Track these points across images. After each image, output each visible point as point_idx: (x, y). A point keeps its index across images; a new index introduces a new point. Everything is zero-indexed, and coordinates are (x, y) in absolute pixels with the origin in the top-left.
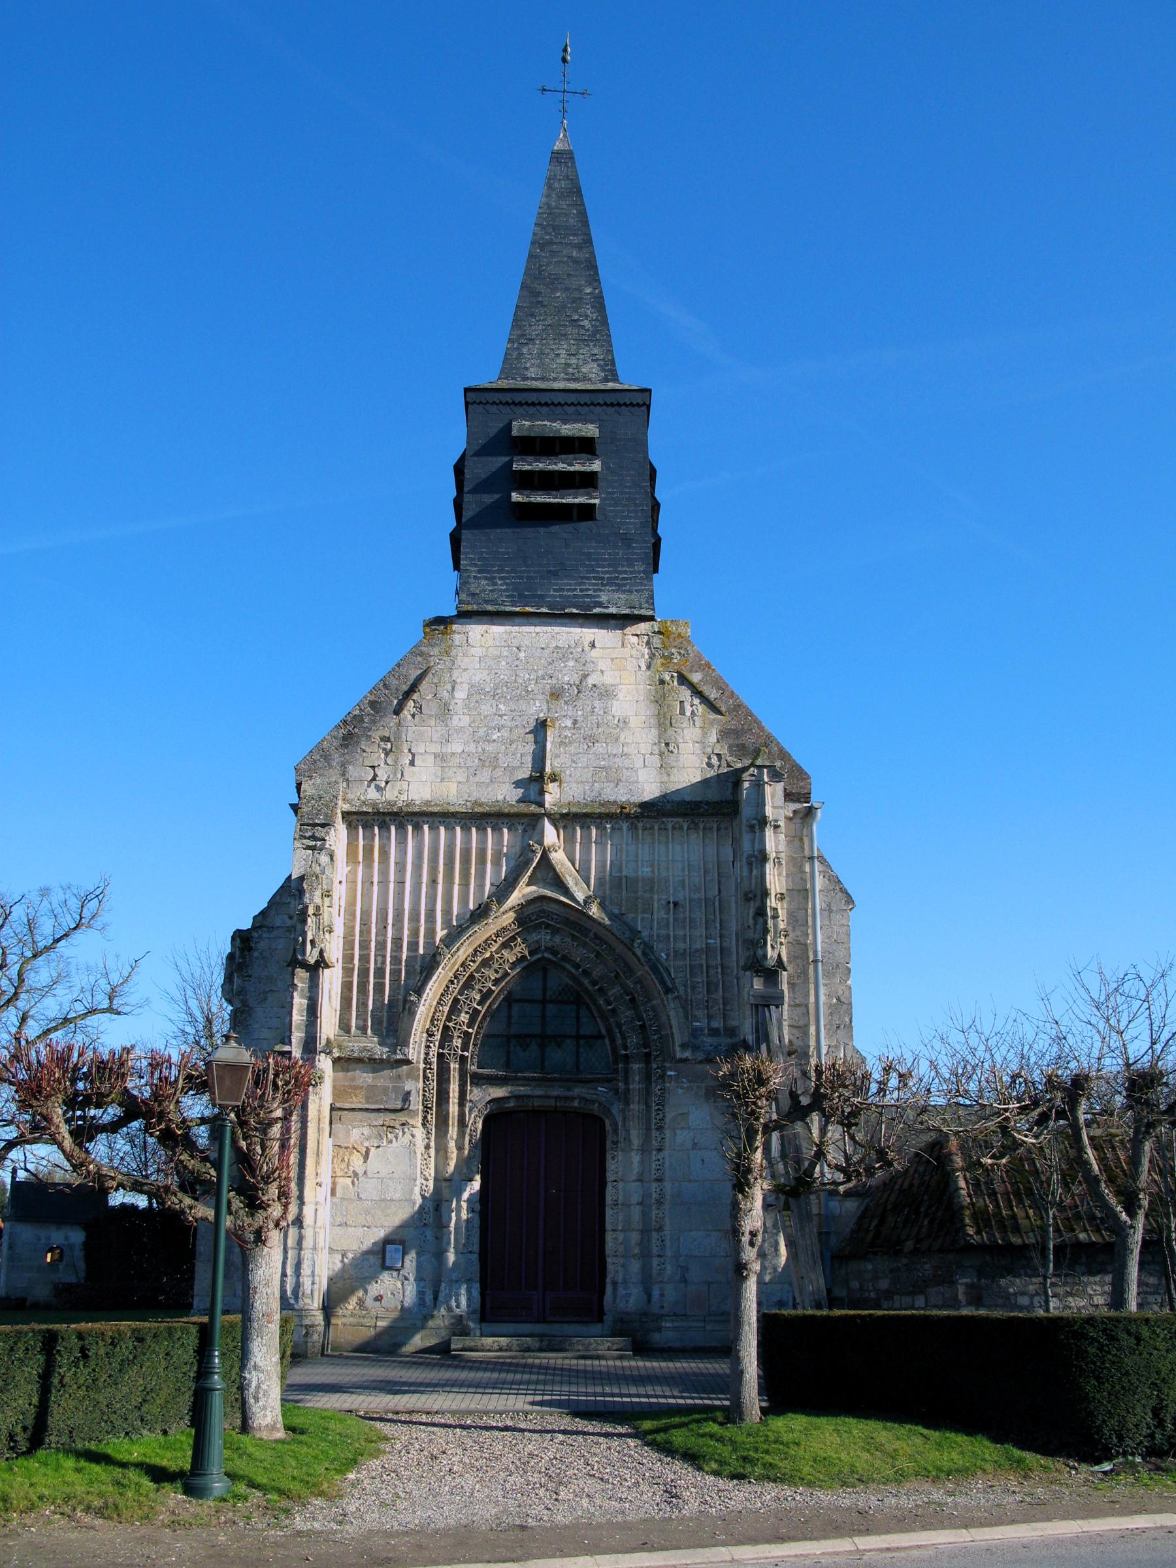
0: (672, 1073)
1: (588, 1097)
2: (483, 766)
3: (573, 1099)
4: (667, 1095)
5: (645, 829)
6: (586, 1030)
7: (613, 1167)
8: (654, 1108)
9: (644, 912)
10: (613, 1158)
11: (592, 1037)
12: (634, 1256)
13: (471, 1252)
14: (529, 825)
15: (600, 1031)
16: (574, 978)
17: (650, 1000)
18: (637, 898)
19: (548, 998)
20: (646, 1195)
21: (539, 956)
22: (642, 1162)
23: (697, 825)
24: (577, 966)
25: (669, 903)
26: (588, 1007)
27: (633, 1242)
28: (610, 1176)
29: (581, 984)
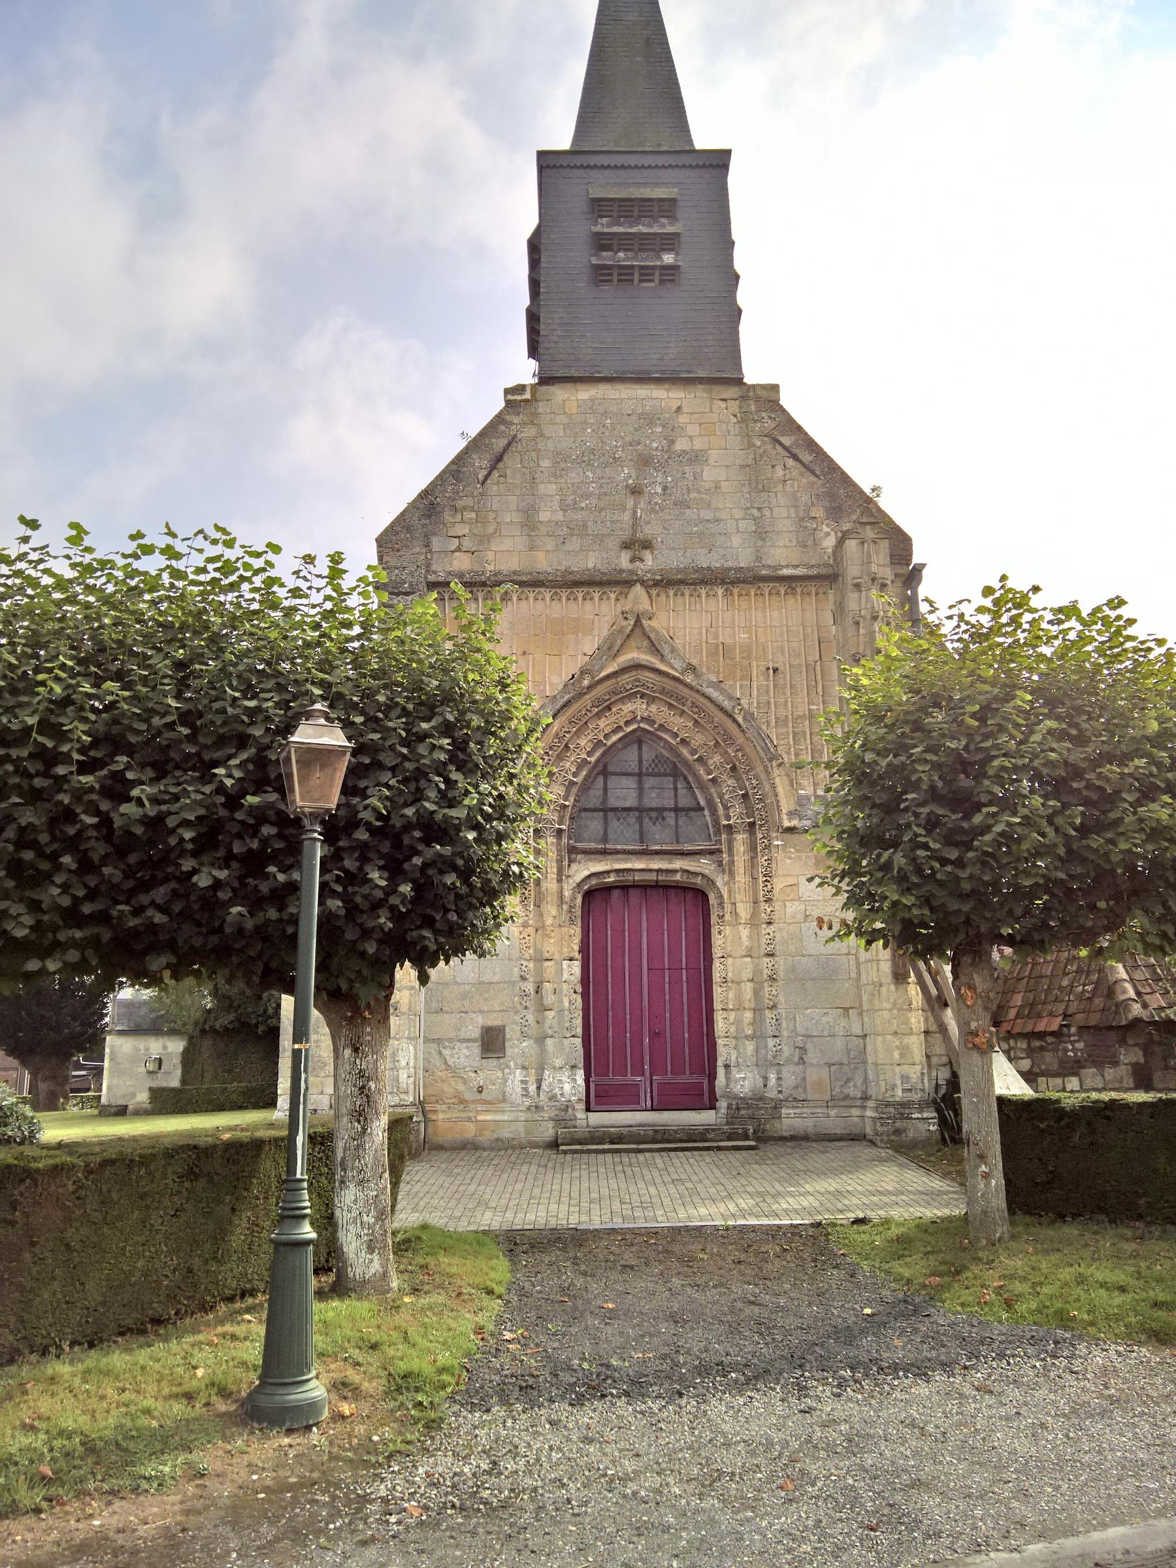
0: (779, 843)
1: (691, 869)
2: (572, 535)
3: (674, 871)
4: (774, 865)
5: (740, 595)
6: (684, 801)
7: (719, 942)
8: (762, 879)
9: (742, 679)
10: (720, 933)
11: (691, 809)
12: (747, 1037)
13: (574, 1036)
14: (621, 593)
15: (698, 803)
16: (671, 748)
17: (752, 769)
18: (734, 665)
19: (644, 770)
20: (757, 971)
21: (634, 726)
22: (750, 937)
23: (794, 589)
24: (676, 735)
25: (768, 669)
26: (685, 778)
27: (746, 1021)
28: (717, 952)
29: (679, 755)
